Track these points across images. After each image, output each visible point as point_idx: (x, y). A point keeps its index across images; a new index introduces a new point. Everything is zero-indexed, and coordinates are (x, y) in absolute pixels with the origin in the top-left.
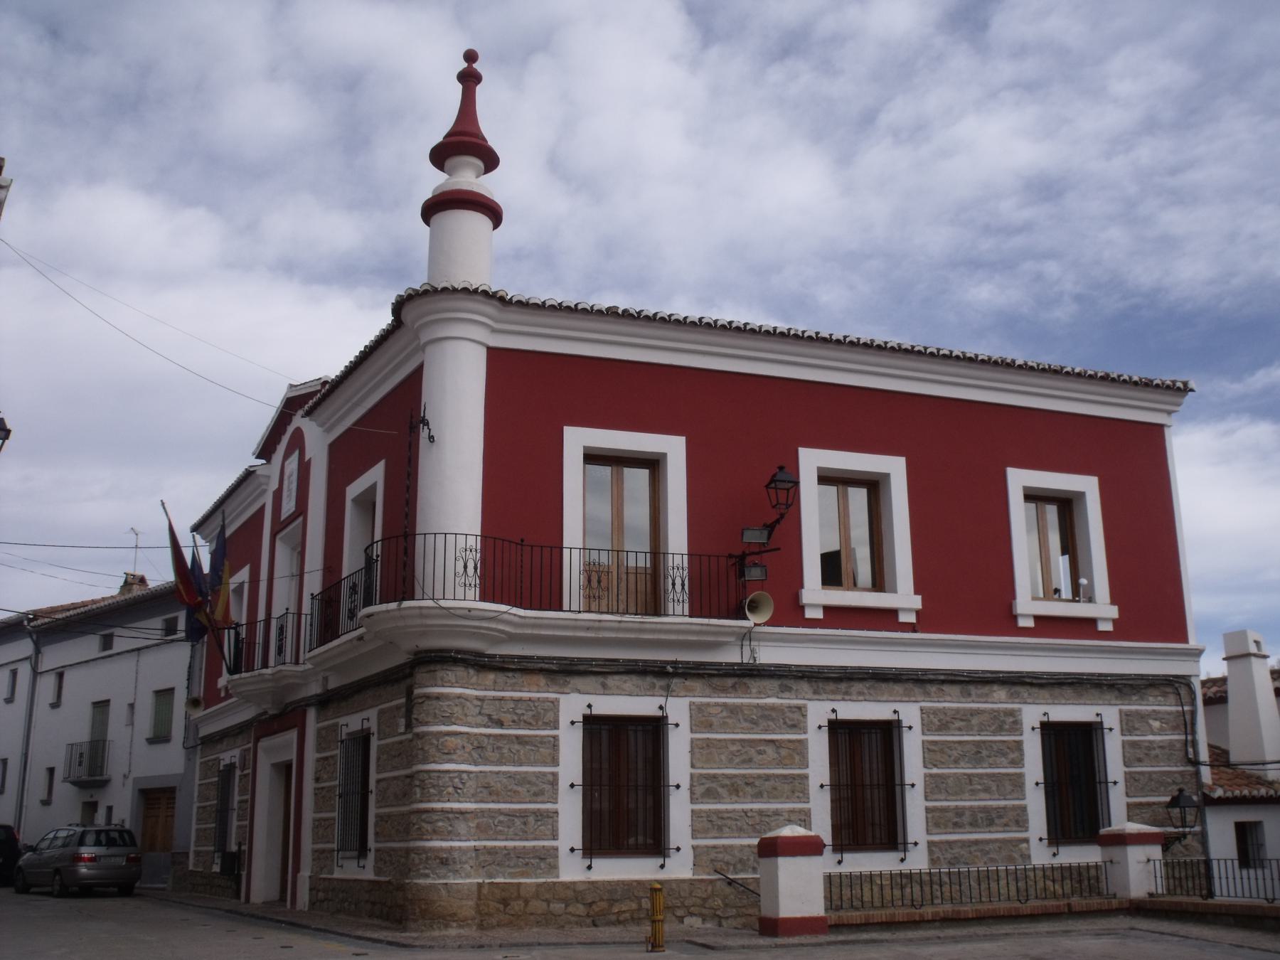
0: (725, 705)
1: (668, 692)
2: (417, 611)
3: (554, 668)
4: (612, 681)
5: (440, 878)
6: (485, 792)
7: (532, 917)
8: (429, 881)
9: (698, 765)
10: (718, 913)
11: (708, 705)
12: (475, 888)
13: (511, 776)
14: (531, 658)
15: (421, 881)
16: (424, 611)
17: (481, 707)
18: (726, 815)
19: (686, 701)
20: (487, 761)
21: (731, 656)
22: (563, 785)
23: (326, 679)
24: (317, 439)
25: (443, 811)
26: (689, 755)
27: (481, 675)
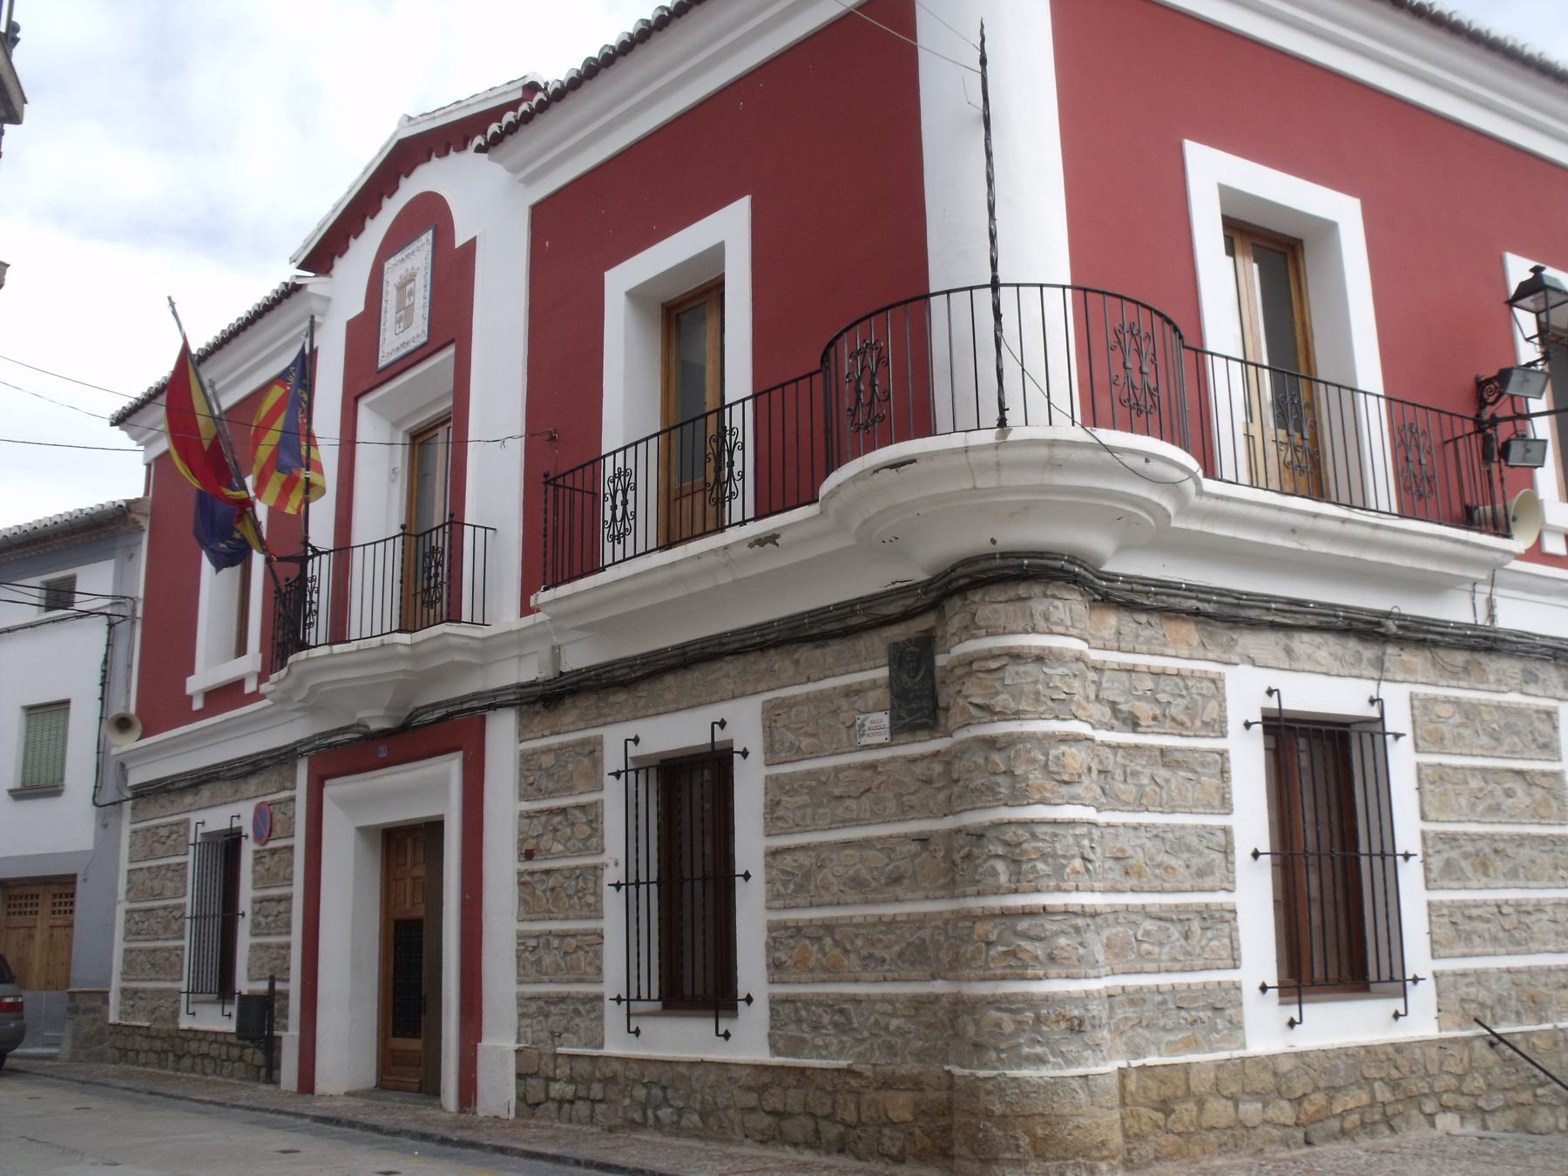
0: (1457, 703)
1: (1381, 672)
2: (1043, 452)
3: (1209, 608)
4: (1304, 643)
5: (1069, 1063)
6: (1117, 867)
7: (1212, 1136)
8: (1047, 1072)
9: (1432, 816)
10: (1481, 1103)
11: (1435, 699)
12: (1114, 1082)
13: (1157, 834)
14: (1176, 586)
15: (1026, 1073)
16: (1060, 453)
17: (1098, 684)
18: (1475, 912)
19: (1406, 689)
20: (1118, 803)
21: (1457, 610)
22: (1242, 854)
23: (556, 653)
24: (489, 205)
25: (1067, 912)
26: (1416, 795)
27: (1096, 616)
